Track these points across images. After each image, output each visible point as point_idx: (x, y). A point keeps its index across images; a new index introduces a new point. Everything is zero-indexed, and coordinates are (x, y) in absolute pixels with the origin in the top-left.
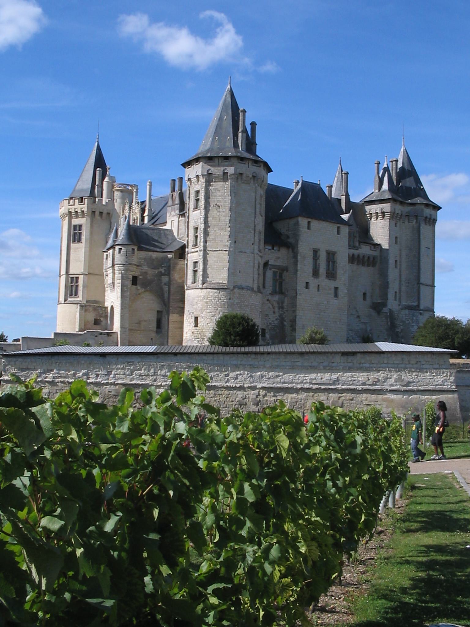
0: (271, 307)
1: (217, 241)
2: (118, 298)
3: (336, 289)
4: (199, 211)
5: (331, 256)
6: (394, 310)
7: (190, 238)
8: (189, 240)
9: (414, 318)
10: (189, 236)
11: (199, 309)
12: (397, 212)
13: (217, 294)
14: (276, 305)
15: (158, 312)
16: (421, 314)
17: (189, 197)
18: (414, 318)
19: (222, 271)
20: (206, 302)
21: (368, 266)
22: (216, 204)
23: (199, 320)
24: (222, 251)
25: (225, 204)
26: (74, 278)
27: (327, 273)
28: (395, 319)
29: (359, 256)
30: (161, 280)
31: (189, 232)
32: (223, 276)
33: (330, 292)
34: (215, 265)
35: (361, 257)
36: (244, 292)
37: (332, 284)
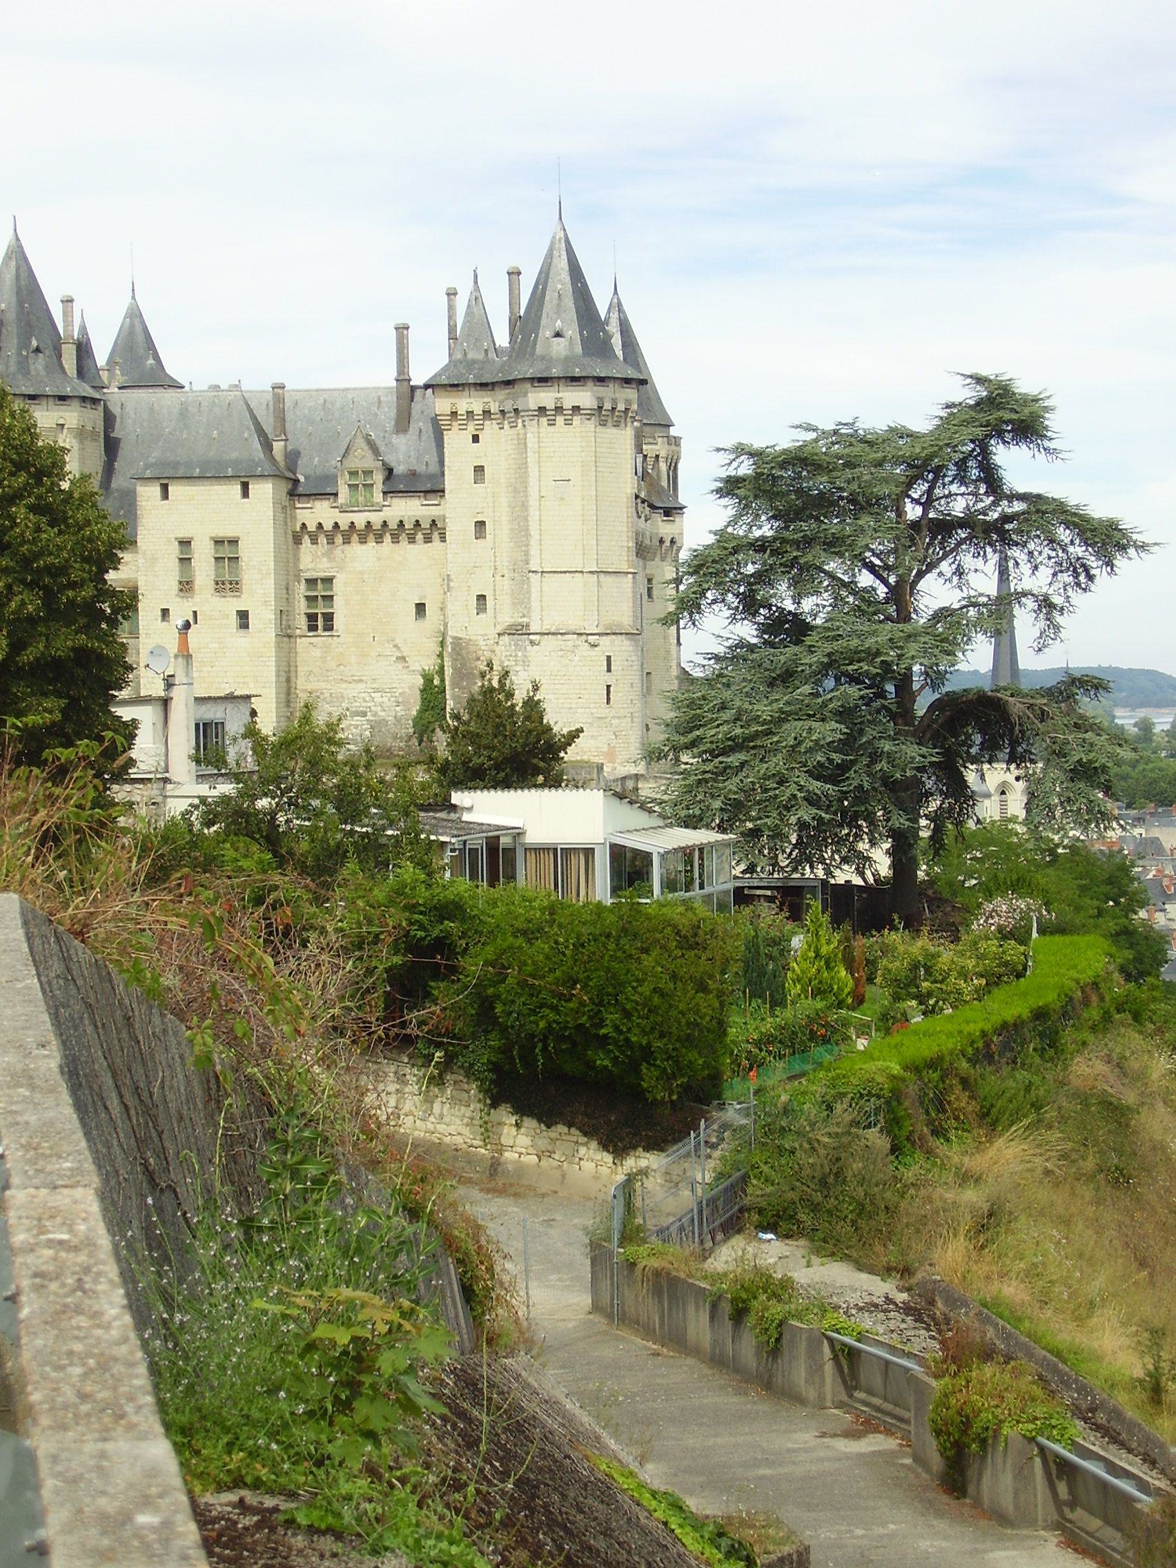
3: (243, 616)
9: (520, 654)
12: (462, 410)
18: (520, 654)
21: (428, 540)
27: (217, 583)
35: (393, 525)
37: (232, 605)
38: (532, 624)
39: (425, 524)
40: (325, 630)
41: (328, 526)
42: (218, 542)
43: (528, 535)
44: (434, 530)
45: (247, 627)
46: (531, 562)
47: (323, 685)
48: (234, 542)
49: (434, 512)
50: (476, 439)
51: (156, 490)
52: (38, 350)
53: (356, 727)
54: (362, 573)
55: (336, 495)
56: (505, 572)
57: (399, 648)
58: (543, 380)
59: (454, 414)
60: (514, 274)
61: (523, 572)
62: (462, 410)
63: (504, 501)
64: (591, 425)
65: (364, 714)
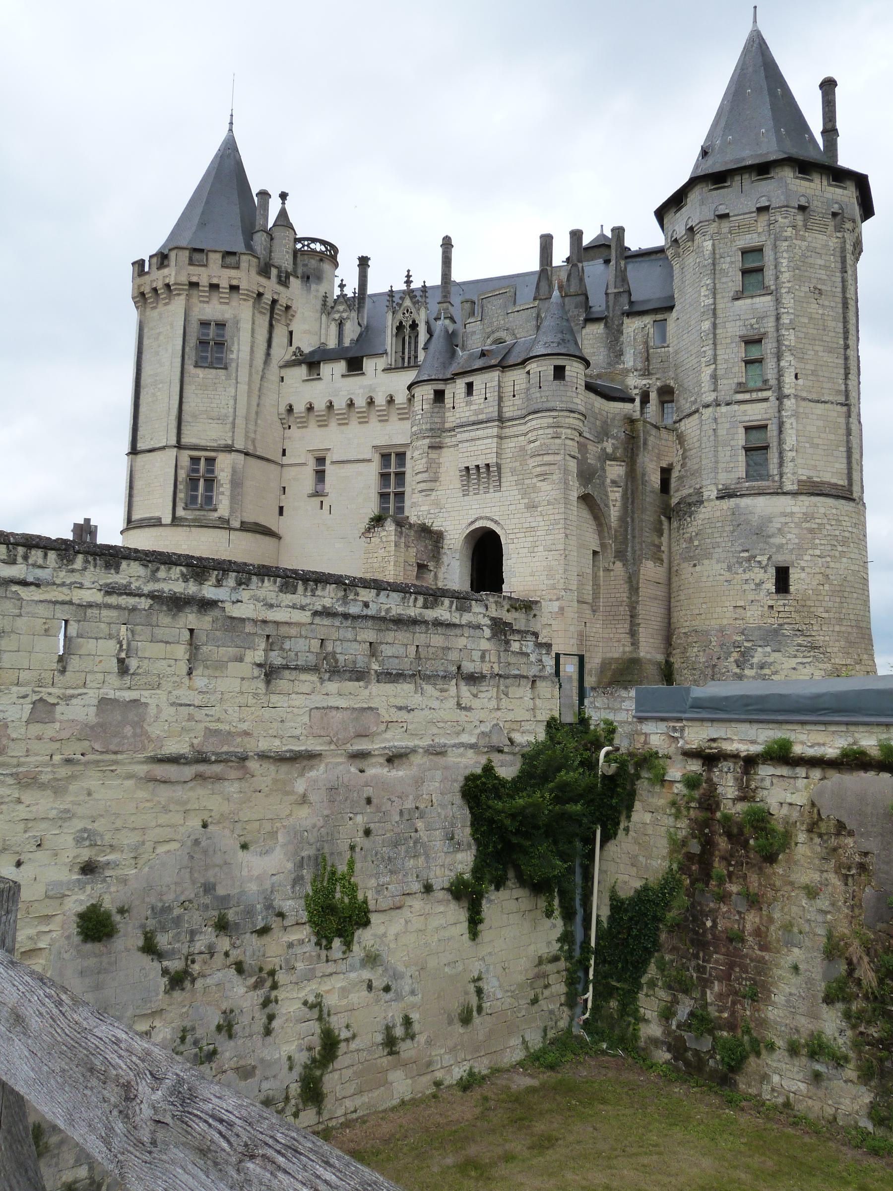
1: (821, 379)
2: (532, 507)
4: (769, 298)
7: (721, 367)
8: (719, 372)
10: (718, 362)
11: (790, 547)
13: (834, 511)
15: (595, 553)
17: (714, 264)
19: (835, 453)
20: (811, 531)
22: (815, 288)
23: (794, 576)
24: (832, 403)
25: (834, 289)
26: (203, 461)
30: (604, 470)
31: (718, 352)
32: (837, 465)
34: (819, 437)
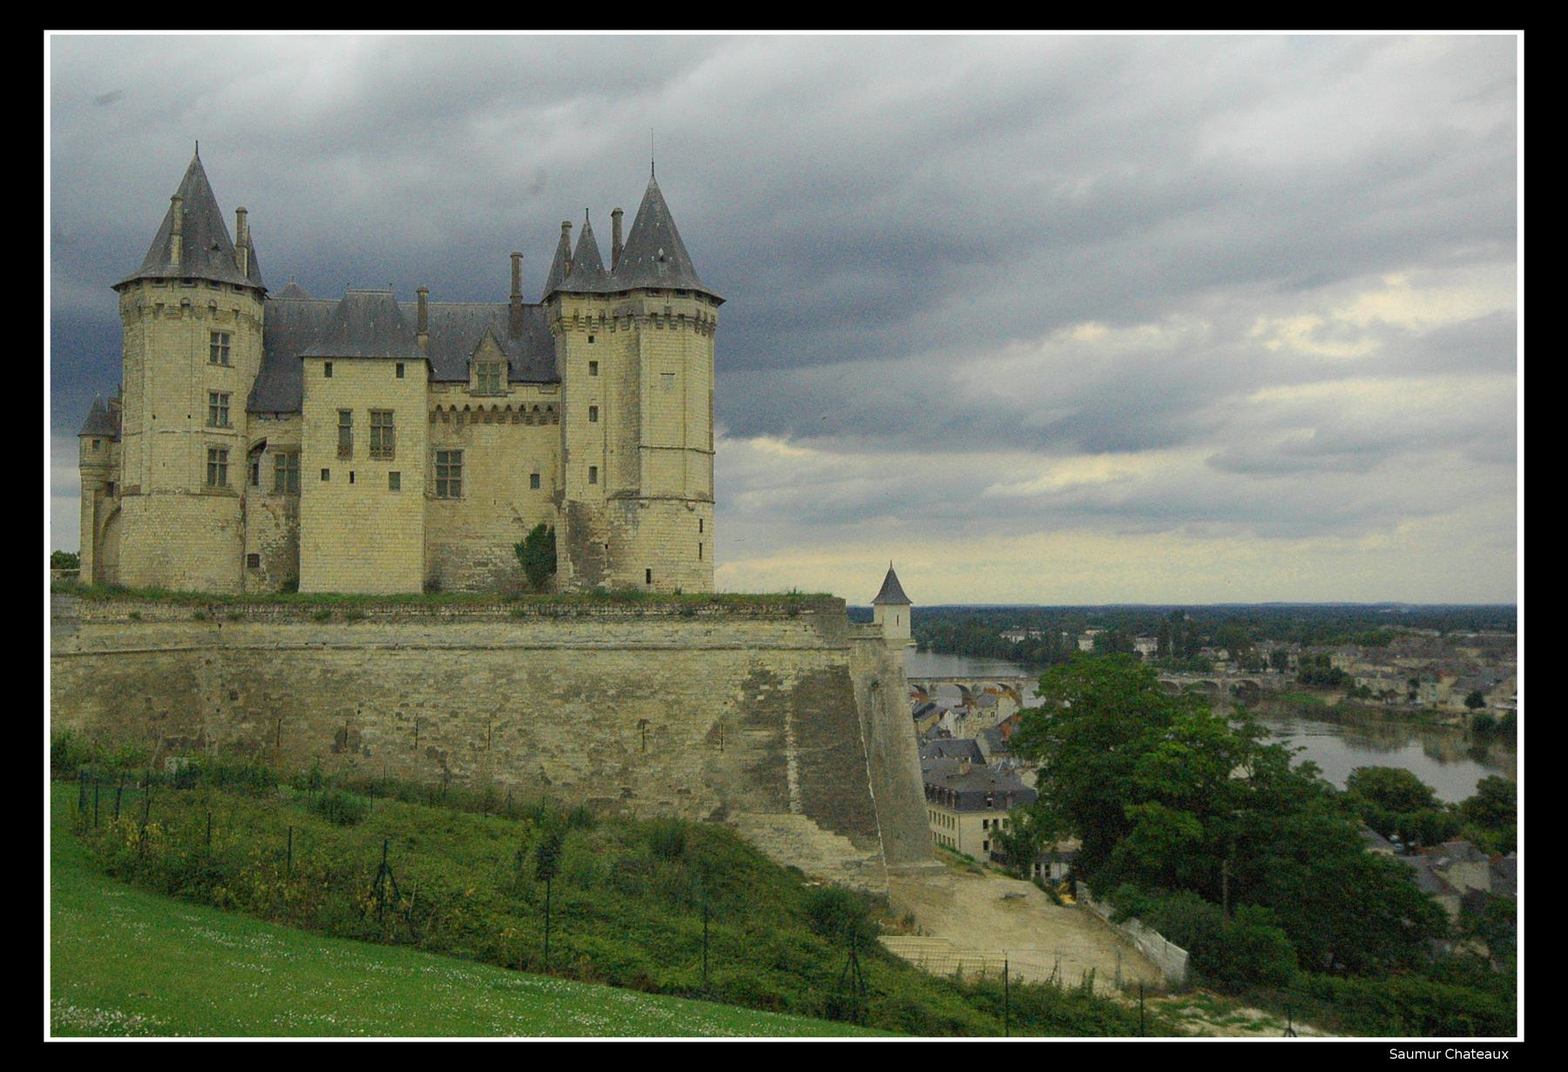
0: (271, 516)
3: (395, 478)
5: (382, 421)
6: (587, 502)
12: (583, 314)
14: (280, 512)
16: (642, 506)
18: (630, 515)
21: (543, 422)
27: (372, 449)
28: (591, 519)
29: (509, 408)
33: (378, 481)
35: (516, 408)
36: (168, 497)
37: (385, 468)
38: (642, 490)
39: (543, 410)
40: (452, 495)
41: (460, 408)
42: (374, 413)
43: (639, 418)
44: (551, 414)
45: (398, 488)
46: (642, 439)
47: (451, 540)
48: (389, 413)
49: (552, 399)
50: (591, 339)
51: (319, 367)
52: (216, 248)
53: (479, 575)
54: (487, 448)
55: (467, 382)
56: (614, 448)
57: (516, 511)
58: (656, 291)
59: (576, 318)
60: (616, 214)
61: (634, 447)
62: (583, 314)
63: (614, 390)
64: (690, 331)
65: (486, 565)
